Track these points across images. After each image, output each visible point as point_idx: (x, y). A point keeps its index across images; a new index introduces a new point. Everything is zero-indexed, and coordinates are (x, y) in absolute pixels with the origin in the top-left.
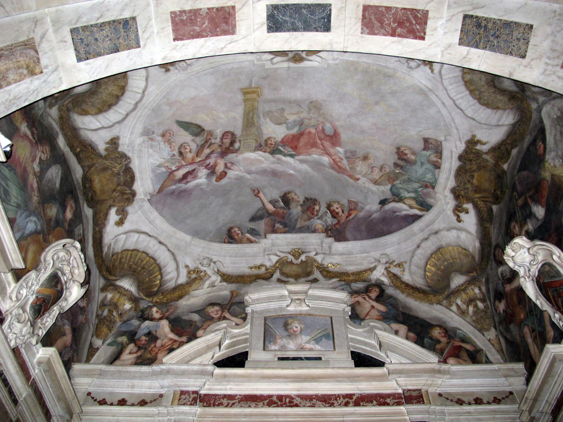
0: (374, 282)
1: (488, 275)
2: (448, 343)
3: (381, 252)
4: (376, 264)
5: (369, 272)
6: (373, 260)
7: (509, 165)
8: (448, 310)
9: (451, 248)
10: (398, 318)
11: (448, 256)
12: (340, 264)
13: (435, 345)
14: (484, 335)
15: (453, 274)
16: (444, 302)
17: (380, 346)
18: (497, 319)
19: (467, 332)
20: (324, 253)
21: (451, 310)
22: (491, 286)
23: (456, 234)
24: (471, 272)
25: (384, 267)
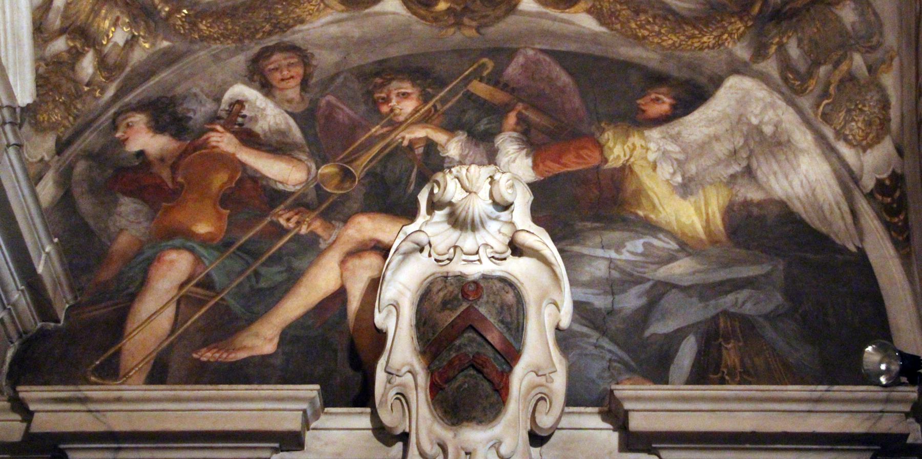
1: (189, 52)
7: (539, 15)
18: (90, 140)
22: (165, 76)
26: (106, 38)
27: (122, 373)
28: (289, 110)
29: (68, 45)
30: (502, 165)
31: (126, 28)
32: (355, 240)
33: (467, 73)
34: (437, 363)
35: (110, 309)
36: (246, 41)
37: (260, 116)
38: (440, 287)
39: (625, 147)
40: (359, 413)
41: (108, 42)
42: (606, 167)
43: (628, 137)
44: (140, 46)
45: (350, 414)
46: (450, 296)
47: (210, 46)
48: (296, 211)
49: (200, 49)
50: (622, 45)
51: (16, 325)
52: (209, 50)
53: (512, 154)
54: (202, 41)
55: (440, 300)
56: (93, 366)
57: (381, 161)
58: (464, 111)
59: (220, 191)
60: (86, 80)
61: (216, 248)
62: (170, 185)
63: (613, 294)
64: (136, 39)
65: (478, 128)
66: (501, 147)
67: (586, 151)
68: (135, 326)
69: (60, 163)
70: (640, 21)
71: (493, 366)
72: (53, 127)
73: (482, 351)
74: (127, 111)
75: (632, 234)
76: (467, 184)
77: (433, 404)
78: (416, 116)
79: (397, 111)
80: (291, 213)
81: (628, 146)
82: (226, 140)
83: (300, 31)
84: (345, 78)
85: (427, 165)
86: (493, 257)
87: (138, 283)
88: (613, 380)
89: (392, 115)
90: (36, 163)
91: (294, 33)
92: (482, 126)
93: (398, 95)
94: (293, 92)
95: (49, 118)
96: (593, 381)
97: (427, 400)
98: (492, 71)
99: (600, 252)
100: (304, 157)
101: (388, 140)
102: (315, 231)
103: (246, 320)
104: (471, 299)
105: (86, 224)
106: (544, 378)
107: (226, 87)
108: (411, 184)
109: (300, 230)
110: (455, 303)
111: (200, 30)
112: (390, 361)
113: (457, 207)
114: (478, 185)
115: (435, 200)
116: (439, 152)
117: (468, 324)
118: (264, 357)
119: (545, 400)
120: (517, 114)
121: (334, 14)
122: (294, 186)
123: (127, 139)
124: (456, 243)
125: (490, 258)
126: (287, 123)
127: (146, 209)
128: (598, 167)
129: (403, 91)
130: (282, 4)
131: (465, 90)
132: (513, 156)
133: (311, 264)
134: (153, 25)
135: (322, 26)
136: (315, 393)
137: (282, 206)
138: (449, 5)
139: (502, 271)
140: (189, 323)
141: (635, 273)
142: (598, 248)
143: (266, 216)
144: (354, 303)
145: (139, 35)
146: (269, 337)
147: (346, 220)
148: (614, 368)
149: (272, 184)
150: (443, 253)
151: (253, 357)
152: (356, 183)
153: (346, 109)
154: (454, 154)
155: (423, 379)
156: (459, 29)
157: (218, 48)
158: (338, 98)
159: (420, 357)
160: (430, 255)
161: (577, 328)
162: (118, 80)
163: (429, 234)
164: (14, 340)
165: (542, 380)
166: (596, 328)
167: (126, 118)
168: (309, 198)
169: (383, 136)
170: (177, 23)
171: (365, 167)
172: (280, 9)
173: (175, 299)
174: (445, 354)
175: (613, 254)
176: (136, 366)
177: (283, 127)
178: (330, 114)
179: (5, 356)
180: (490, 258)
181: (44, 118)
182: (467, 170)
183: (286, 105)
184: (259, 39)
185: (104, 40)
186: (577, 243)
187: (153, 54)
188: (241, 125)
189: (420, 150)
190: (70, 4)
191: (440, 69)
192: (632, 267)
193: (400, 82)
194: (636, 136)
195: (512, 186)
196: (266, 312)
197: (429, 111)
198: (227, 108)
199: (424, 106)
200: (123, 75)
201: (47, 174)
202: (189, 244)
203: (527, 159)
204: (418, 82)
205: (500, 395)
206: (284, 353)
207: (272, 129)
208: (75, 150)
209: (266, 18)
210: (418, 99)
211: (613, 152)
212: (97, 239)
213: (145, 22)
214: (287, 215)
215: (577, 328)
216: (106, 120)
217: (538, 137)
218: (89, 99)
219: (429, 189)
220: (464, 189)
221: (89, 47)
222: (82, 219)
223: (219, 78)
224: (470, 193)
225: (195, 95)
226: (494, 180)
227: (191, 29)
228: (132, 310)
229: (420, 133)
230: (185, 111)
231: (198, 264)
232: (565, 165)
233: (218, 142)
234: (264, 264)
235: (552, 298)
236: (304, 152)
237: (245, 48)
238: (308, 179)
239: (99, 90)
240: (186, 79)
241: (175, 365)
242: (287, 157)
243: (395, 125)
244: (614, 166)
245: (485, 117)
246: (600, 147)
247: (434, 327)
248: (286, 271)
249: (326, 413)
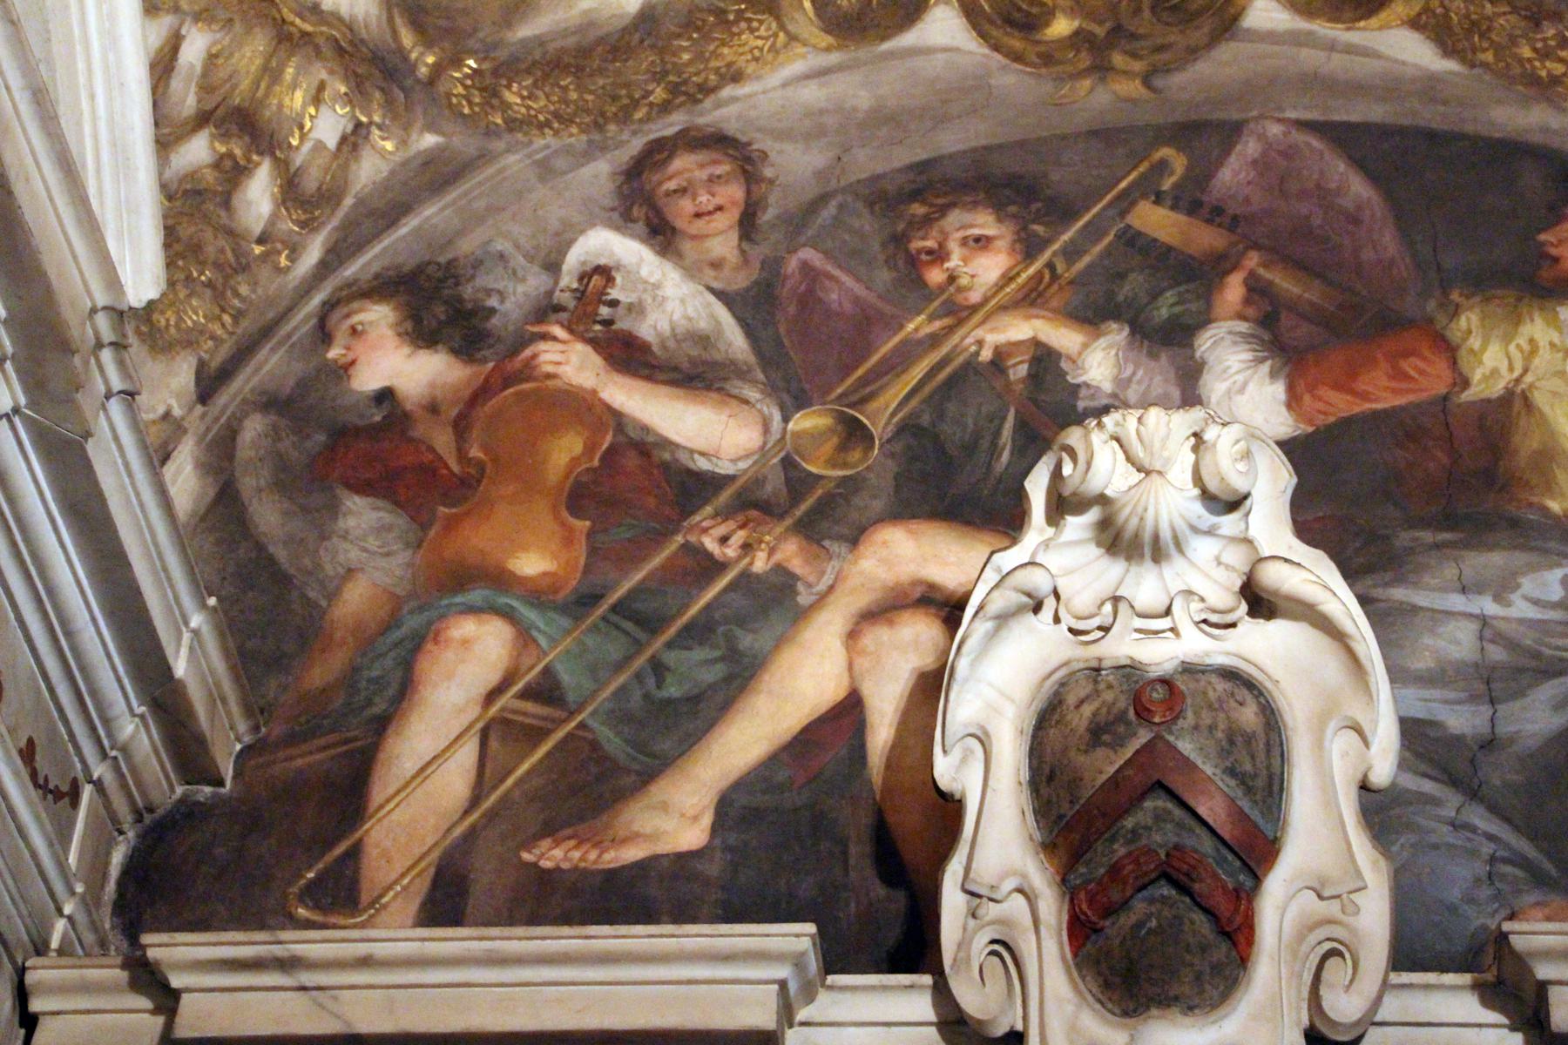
1: (484, 157)
22: (431, 214)
24: (418, 26)
26: (297, 131)
27: (365, 898)
28: (716, 285)
29: (214, 149)
30: (1213, 400)
32: (878, 584)
33: (1123, 184)
34: (1083, 870)
35: (332, 752)
36: (612, 127)
37: (650, 301)
38: (1082, 693)
39: (1512, 348)
40: (906, 987)
41: (303, 137)
42: (1467, 396)
43: (1518, 322)
44: (373, 147)
45: (885, 988)
46: (1109, 713)
47: (531, 142)
48: (741, 518)
49: (508, 151)
50: (1499, 102)
51: (130, 796)
52: (526, 151)
53: (1237, 372)
54: (511, 130)
55: (1084, 724)
56: (303, 882)
57: (931, 397)
58: (1122, 276)
59: (567, 477)
60: (257, 229)
61: (564, 609)
62: (456, 468)
63: (1492, 702)
64: (364, 132)
65: (1155, 313)
66: (1211, 359)
67: (1412, 359)
68: (391, 790)
69: (209, 419)
70: (1544, 40)
71: (1215, 876)
72: (188, 341)
73: (1189, 842)
74: (352, 298)
75: (1534, 558)
76: (1139, 452)
77: (1077, 965)
78: (1008, 290)
79: (964, 281)
80: (731, 525)
81: (1518, 346)
82: (574, 359)
83: (734, 99)
84: (841, 207)
85: (1035, 402)
86: (1205, 621)
87: (391, 692)
88: (1501, 906)
89: (952, 289)
90: (154, 422)
91: (718, 105)
92: (1163, 310)
93: (964, 242)
94: (722, 242)
95: (180, 320)
96: (1452, 909)
97: (1064, 959)
98: (1186, 177)
99: (1457, 602)
100: (753, 394)
101: (944, 350)
102: (785, 564)
103: (638, 773)
104: (1157, 720)
105: (272, 561)
106: (1336, 902)
107: (567, 236)
108: (1003, 449)
109: (751, 564)
110: (1121, 729)
111: (506, 106)
112: (974, 865)
113: (1119, 505)
114: (1166, 454)
115: (1066, 492)
116: (1063, 374)
117: (1155, 779)
118: (682, 858)
119: (1340, 954)
120: (1246, 283)
121: (809, 56)
122: (734, 461)
123: (353, 363)
124: (1117, 589)
125: (1197, 623)
126: (712, 316)
127: (401, 521)
128: (1445, 398)
129: (977, 232)
130: (690, 38)
131: (1122, 225)
132: (1240, 378)
133: (780, 643)
134: (396, 91)
135: (784, 85)
136: (805, 944)
137: (709, 509)
138: (1076, 24)
139: (1228, 654)
140: (510, 781)
141: (1548, 652)
142: (1454, 591)
143: (676, 531)
144: (881, 733)
145: (371, 123)
146: (691, 812)
147: (854, 540)
148: (1503, 877)
149: (683, 457)
150: (1086, 613)
151: (656, 858)
152: (876, 452)
153: (847, 280)
154: (1099, 378)
155: (1051, 906)
156: (1103, 79)
157: (547, 147)
158: (827, 254)
159: (1042, 856)
160: (1057, 620)
161: (1411, 782)
162: (329, 227)
163: (1054, 571)
164: (126, 827)
165: (1333, 908)
166: (1454, 782)
167: (348, 316)
168: (769, 488)
169: (935, 340)
170: (455, 92)
171: (893, 414)
172: (685, 49)
173: (480, 725)
174: (1099, 846)
175: (1488, 606)
176: (396, 882)
177: (703, 325)
178: (810, 291)
179: (107, 864)
180: (1197, 623)
181: (168, 320)
182: (1140, 419)
183: (710, 273)
184: (641, 121)
186: (1400, 580)
187: (405, 164)
188: (608, 323)
189: (1019, 371)
190: (216, 56)
191: (1059, 177)
192: (1537, 635)
193: (969, 210)
194: (1538, 320)
195: (1247, 455)
196: (679, 756)
197: (1039, 276)
198: (575, 285)
199: (1026, 268)
200: (341, 213)
201: (180, 448)
202: (503, 600)
203: (1272, 383)
204: (1012, 209)
205: (1235, 944)
206: (728, 848)
207: (677, 331)
208: (240, 390)
209: (655, 73)
210: (1012, 251)
211: (1481, 362)
212: (295, 594)
213: (382, 90)
214: (721, 530)
215: (1411, 782)
216: (305, 321)
217: (1298, 331)
218: (264, 273)
219: (1052, 468)
220: (1133, 464)
221: (261, 154)
222: (260, 548)
223: (555, 214)
224: (1148, 473)
225: (502, 256)
226: (1204, 442)
227: (486, 103)
228: (382, 756)
229: (1019, 329)
230: (480, 295)
231: (525, 645)
232: (1365, 396)
233: (559, 363)
234: (670, 645)
235: (1350, 714)
236: (754, 382)
237: (610, 142)
238: (765, 443)
239: (286, 252)
240: (481, 220)
241: (485, 877)
242: (714, 395)
243: (959, 313)
244: (1487, 394)
245: (1171, 287)
246: (1449, 350)
247: (1075, 782)
248: (722, 659)
249: (831, 988)
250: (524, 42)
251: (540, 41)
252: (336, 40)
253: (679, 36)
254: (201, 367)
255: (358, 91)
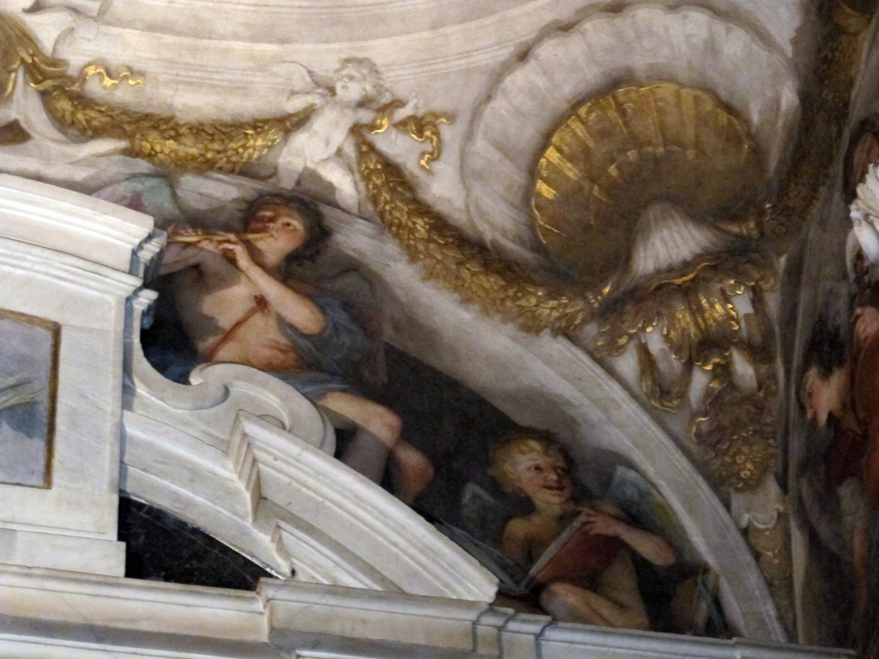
0: (287, 183)
1: (804, 243)
2: (564, 519)
3: (345, 49)
4: (314, 99)
5: (275, 135)
6: (300, 80)
8: (599, 371)
9: (666, 91)
10: (366, 374)
11: (646, 126)
12: (141, 74)
13: (507, 519)
14: (727, 506)
15: (654, 211)
16: (591, 329)
17: (260, 499)
18: (796, 446)
19: (661, 482)
20: (74, 10)
21: (611, 372)
22: (804, 297)
23: (704, 34)
24: (733, 218)
25: (348, 120)
31: (739, 290)
41: (738, 323)
60: (754, 384)
134: (756, 256)
185: (733, 326)
213: (748, 261)
221: (727, 350)
250: (778, 171)
251: (781, 162)
252: (708, 266)
253: (821, 92)
254: (776, 475)
255: (740, 276)
